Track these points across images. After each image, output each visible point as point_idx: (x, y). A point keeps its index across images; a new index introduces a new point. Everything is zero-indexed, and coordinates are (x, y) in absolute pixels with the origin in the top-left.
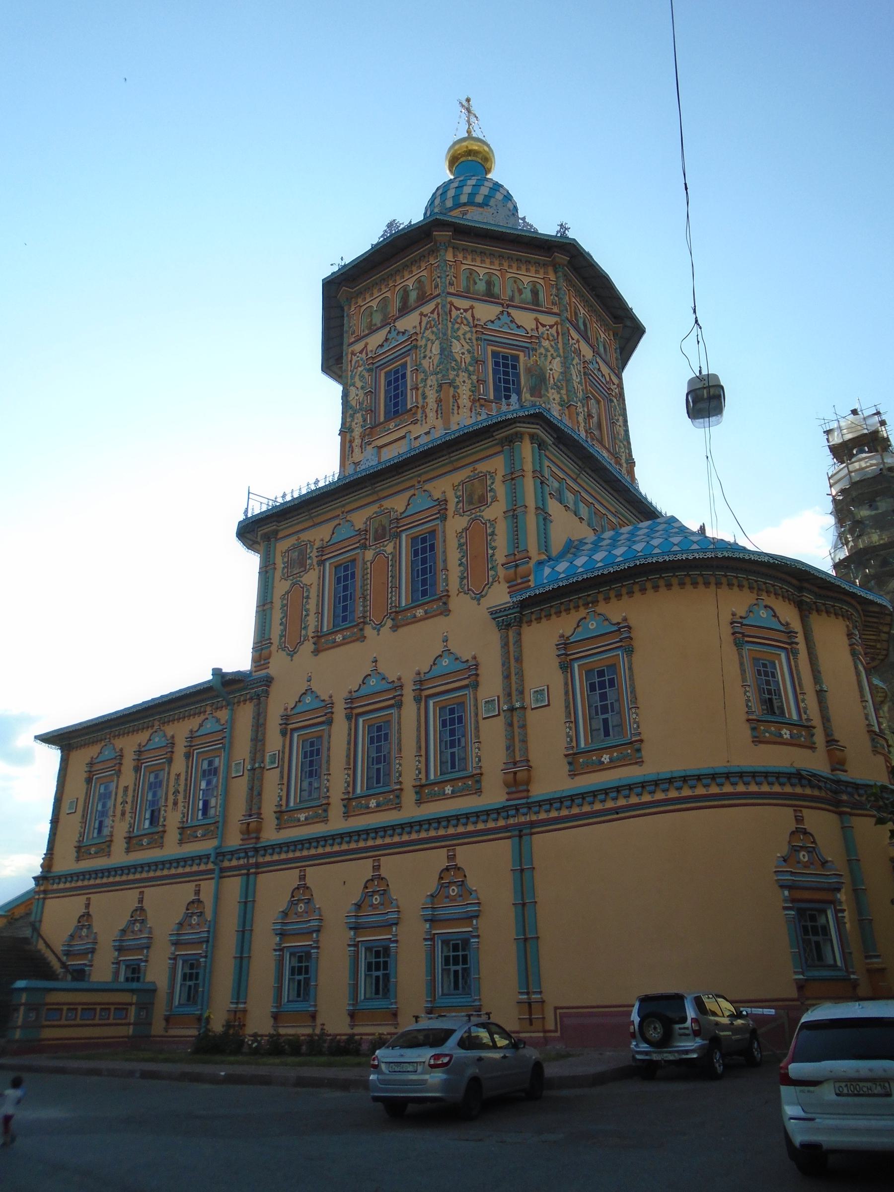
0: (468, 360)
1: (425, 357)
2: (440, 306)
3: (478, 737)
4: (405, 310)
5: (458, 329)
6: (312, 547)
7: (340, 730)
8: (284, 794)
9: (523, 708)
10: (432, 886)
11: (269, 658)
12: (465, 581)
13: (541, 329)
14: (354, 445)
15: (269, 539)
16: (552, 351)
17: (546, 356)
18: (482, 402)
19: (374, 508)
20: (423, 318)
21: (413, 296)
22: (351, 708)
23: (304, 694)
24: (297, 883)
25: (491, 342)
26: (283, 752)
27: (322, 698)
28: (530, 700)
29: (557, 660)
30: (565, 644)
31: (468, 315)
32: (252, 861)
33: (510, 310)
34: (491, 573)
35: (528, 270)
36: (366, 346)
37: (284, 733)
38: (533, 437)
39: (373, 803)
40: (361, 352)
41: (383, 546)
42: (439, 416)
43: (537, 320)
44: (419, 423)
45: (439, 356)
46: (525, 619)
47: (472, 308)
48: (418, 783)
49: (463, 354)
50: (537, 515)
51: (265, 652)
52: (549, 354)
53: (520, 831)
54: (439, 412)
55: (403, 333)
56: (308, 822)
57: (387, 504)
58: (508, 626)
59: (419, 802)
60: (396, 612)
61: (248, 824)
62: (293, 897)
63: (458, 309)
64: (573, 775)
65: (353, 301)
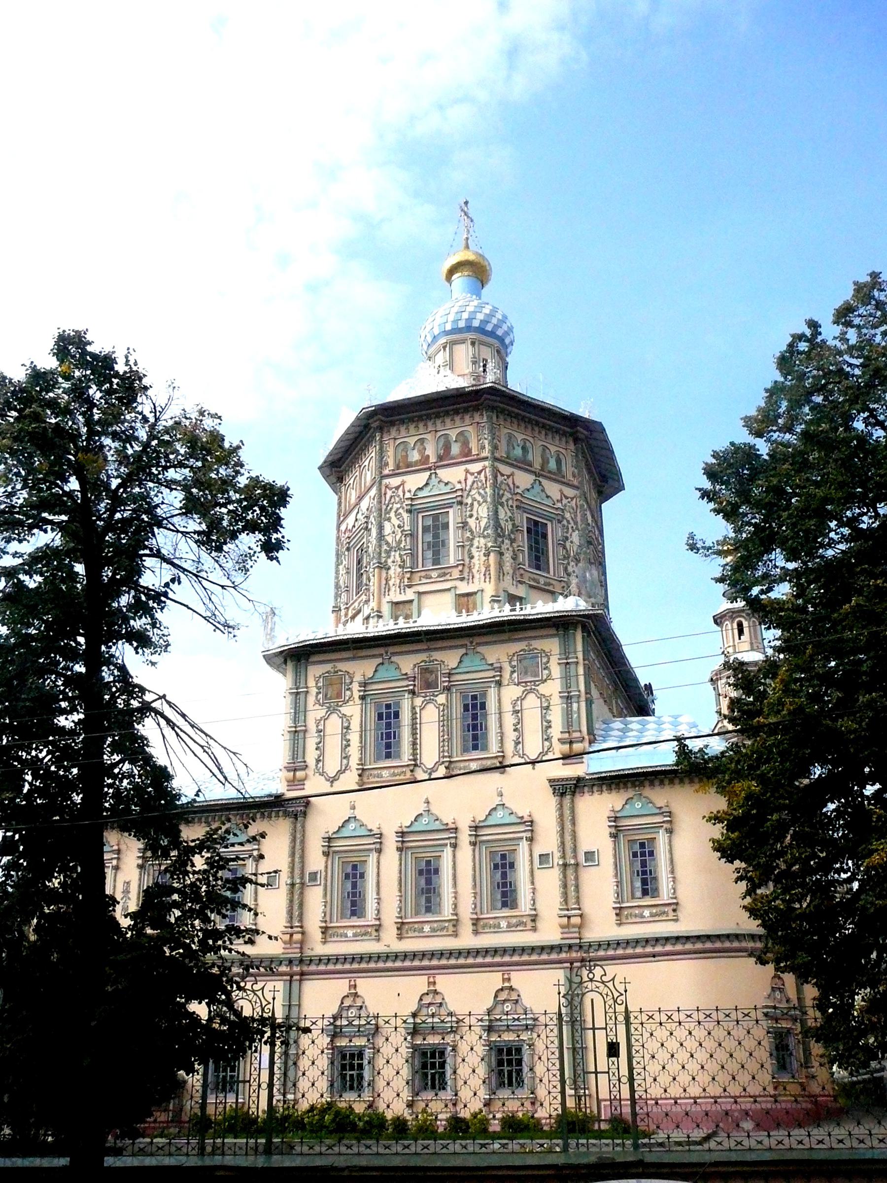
0: (510, 527)
1: (471, 516)
2: (487, 470)
4: (445, 458)
5: (503, 495)
6: (351, 678)
7: (391, 858)
9: (577, 865)
10: (490, 1003)
11: (305, 779)
12: (520, 746)
13: (565, 501)
14: (391, 583)
15: (299, 660)
16: (572, 524)
17: (568, 529)
18: (522, 571)
19: (423, 656)
20: (468, 475)
21: (455, 449)
22: (403, 842)
24: (346, 991)
25: (525, 511)
26: (326, 871)
28: (581, 858)
29: (608, 830)
30: (616, 817)
31: (510, 481)
32: (296, 969)
33: (541, 479)
34: (547, 744)
35: (553, 437)
36: (403, 483)
37: (326, 854)
38: (585, 628)
39: (427, 928)
40: (397, 488)
41: (433, 695)
42: (487, 580)
43: (562, 493)
44: (465, 582)
45: (486, 520)
46: (578, 790)
47: (512, 474)
48: (475, 916)
49: (507, 521)
50: (587, 700)
51: (299, 774)
52: (570, 526)
53: (572, 964)
54: (488, 577)
55: (446, 484)
56: (357, 937)
57: (438, 655)
58: (562, 795)
59: (476, 932)
60: (450, 762)
61: (291, 935)
62: (342, 1003)
63: (503, 475)
64: (620, 925)
65: (386, 429)
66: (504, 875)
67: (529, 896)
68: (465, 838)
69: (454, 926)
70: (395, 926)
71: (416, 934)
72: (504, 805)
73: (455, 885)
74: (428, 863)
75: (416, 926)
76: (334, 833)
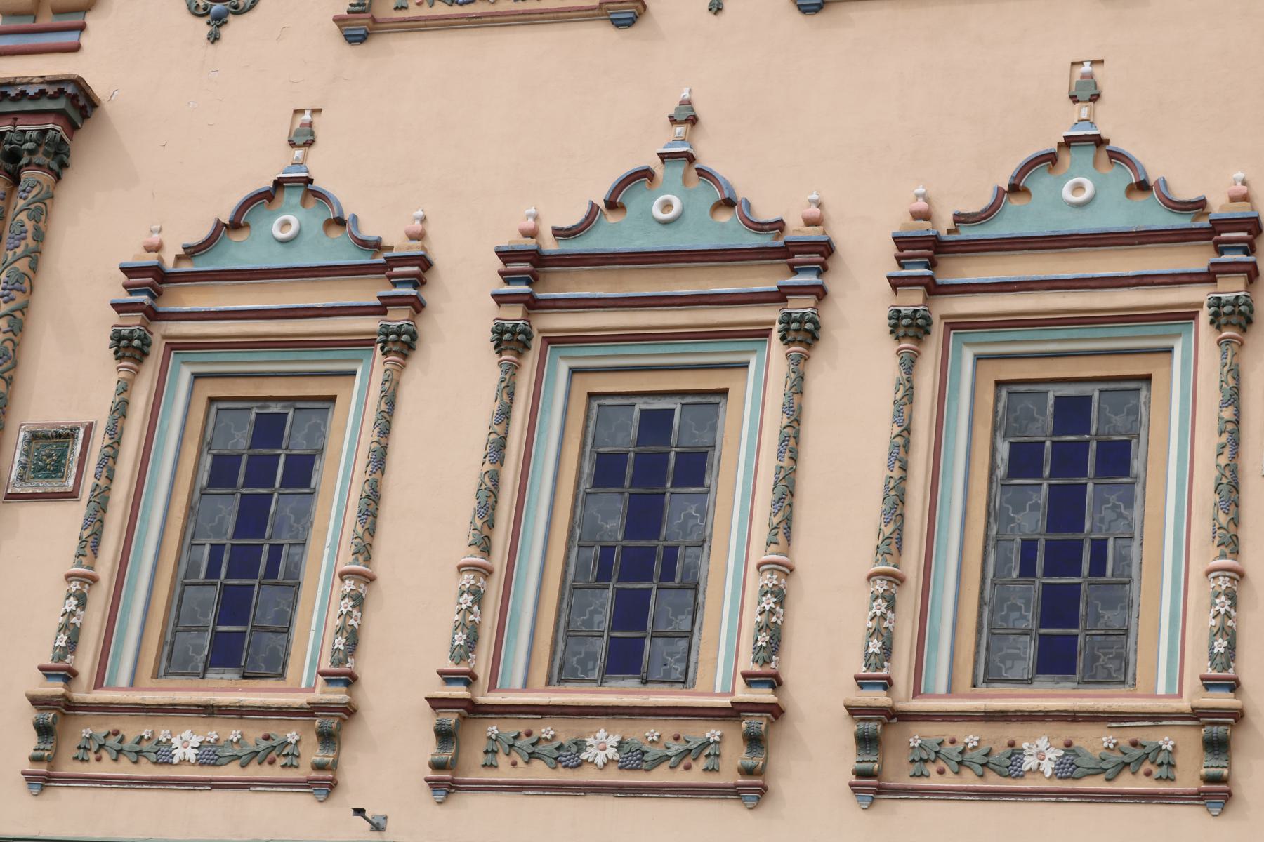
3: (1231, 543)
8: (93, 622)
23: (267, 197)
27: (368, 231)
37: (129, 348)
39: (602, 742)
48: (877, 698)
66: (1065, 510)
67: (1201, 621)
68: (862, 296)
69: (755, 741)
70: (427, 722)
71: (540, 772)
72: (1099, 141)
73: (784, 528)
74: (655, 423)
75: (545, 729)
76: (191, 252)
